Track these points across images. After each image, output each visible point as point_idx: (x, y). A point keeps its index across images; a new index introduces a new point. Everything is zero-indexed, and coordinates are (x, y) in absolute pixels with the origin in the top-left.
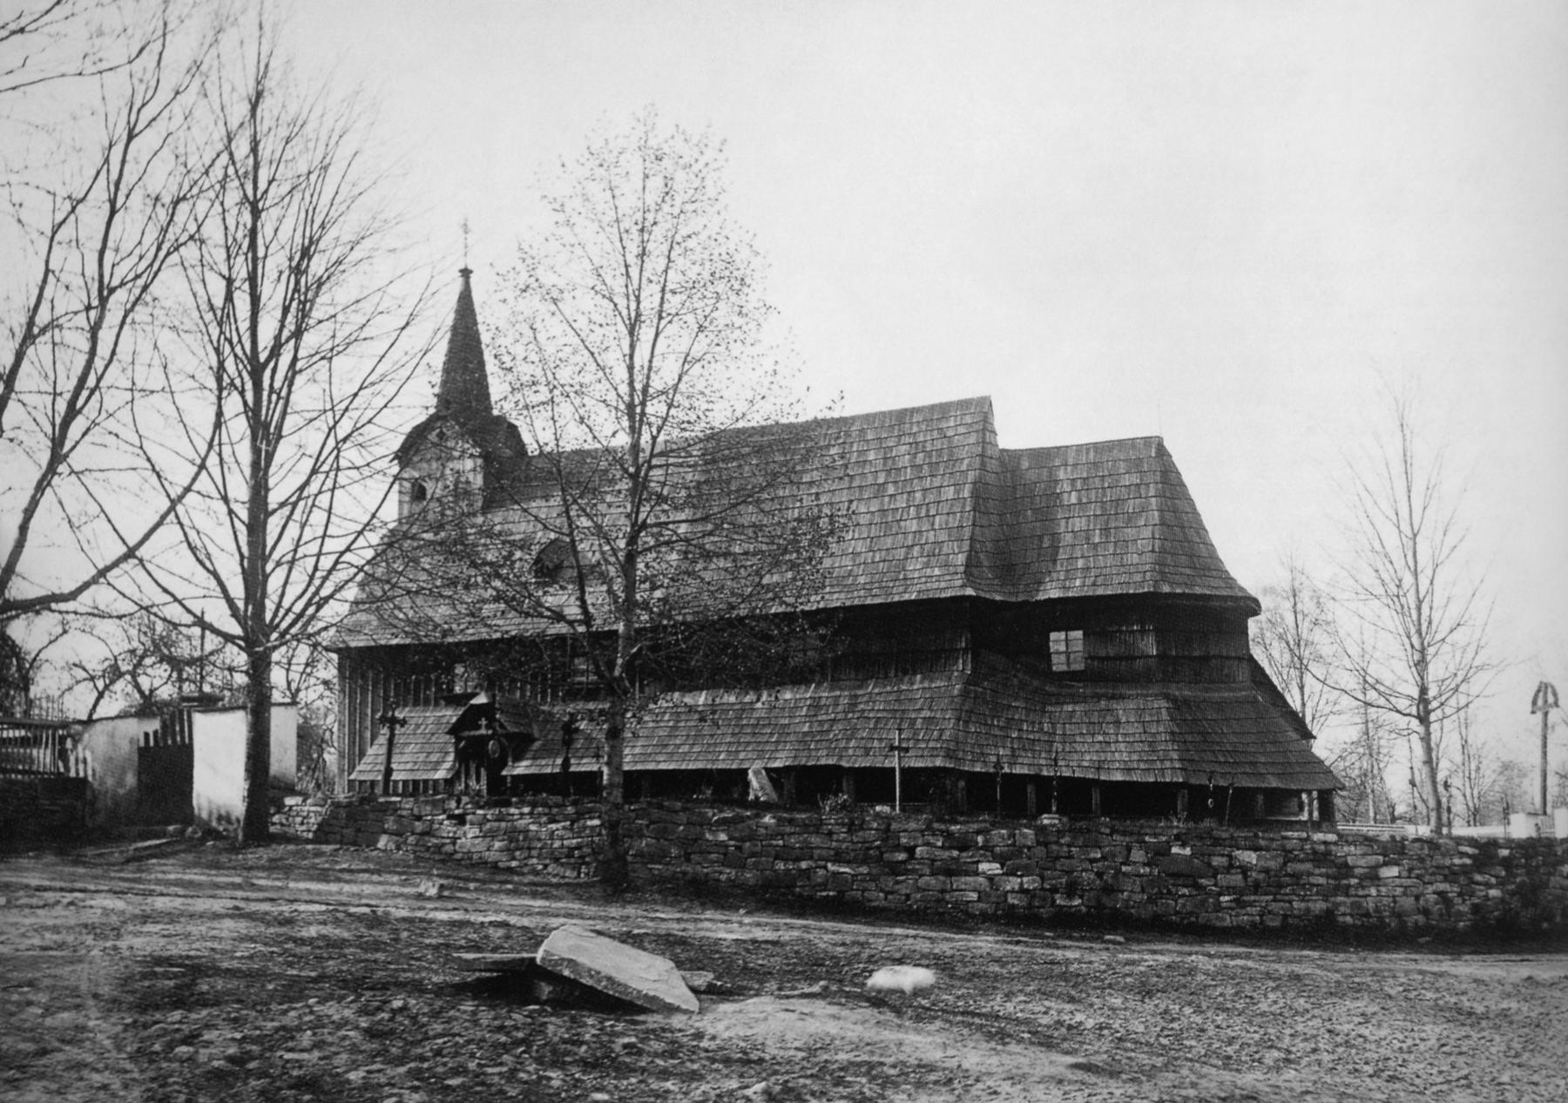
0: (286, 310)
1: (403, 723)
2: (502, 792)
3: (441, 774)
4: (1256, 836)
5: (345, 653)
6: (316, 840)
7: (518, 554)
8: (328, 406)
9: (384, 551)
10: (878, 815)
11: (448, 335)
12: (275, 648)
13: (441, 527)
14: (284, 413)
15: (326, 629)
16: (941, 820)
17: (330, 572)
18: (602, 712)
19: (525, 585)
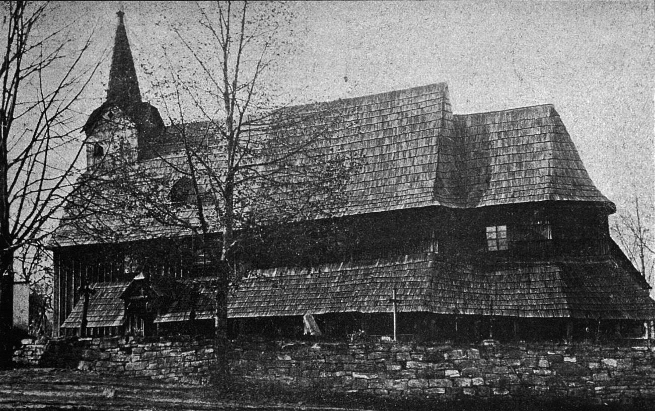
0: (10, 40)
1: (94, 292)
2: (153, 334)
3: (116, 324)
4: (616, 350)
5: (60, 253)
6: (41, 365)
7: (161, 187)
8: (41, 100)
9: (79, 188)
10: (382, 342)
11: (112, 53)
12: (16, 248)
13: (113, 172)
14: (14, 104)
15: (45, 236)
16: (421, 345)
17: (46, 202)
18: (214, 283)
19: (166, 206)
